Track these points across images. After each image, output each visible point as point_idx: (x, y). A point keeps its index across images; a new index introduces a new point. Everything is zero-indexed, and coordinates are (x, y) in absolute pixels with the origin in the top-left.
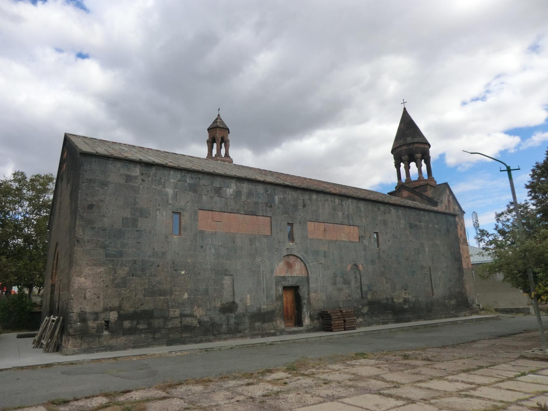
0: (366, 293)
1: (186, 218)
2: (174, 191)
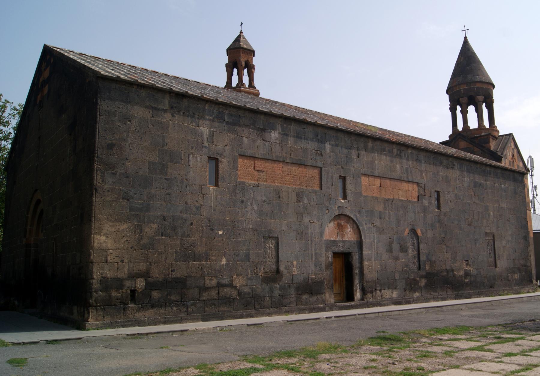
1: (224, 165)
2: (210, 131)
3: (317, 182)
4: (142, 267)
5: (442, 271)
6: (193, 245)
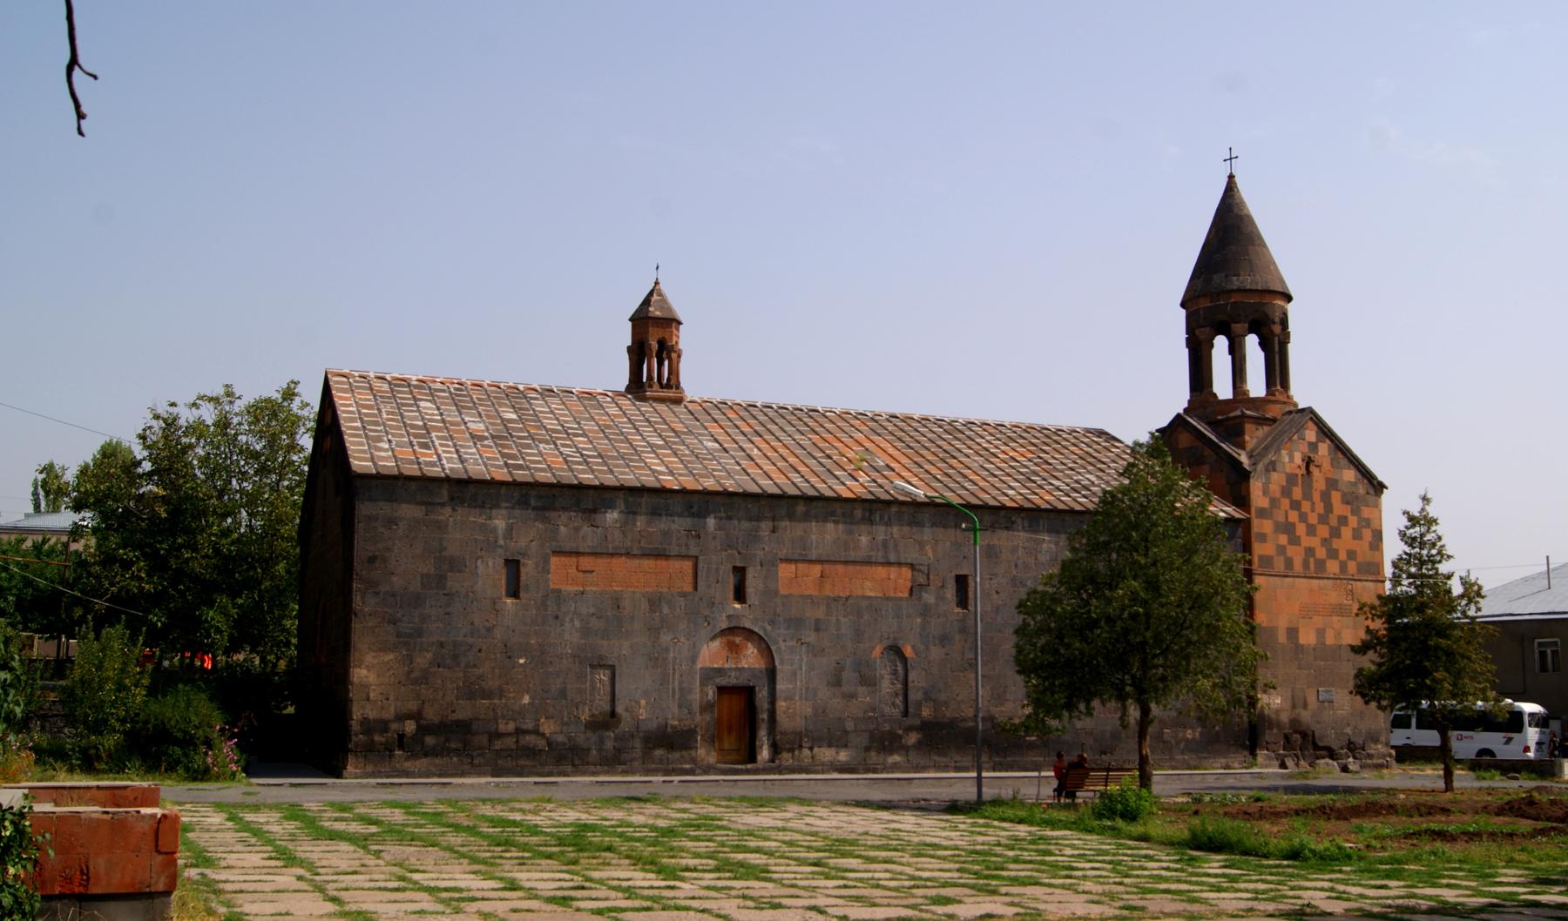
0: (919, 705)
3: (689, 579)
4: (412, 706)
5: (965, 720)
6: (481, 677)
